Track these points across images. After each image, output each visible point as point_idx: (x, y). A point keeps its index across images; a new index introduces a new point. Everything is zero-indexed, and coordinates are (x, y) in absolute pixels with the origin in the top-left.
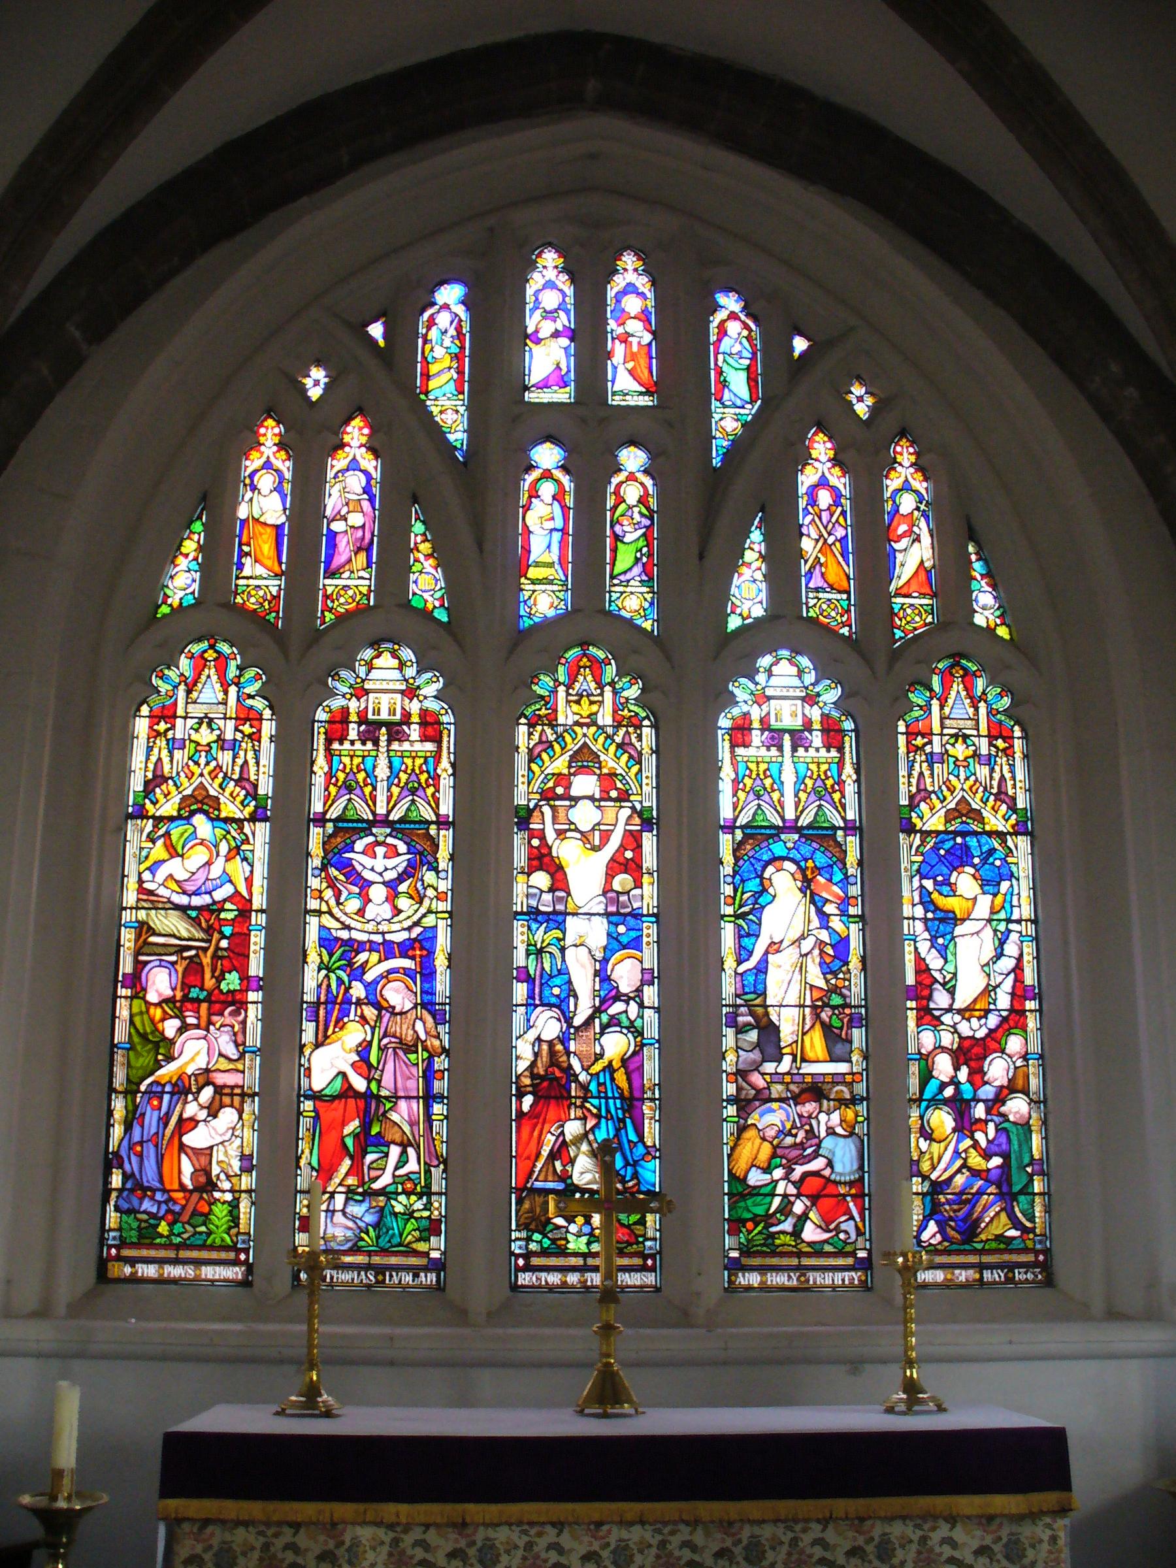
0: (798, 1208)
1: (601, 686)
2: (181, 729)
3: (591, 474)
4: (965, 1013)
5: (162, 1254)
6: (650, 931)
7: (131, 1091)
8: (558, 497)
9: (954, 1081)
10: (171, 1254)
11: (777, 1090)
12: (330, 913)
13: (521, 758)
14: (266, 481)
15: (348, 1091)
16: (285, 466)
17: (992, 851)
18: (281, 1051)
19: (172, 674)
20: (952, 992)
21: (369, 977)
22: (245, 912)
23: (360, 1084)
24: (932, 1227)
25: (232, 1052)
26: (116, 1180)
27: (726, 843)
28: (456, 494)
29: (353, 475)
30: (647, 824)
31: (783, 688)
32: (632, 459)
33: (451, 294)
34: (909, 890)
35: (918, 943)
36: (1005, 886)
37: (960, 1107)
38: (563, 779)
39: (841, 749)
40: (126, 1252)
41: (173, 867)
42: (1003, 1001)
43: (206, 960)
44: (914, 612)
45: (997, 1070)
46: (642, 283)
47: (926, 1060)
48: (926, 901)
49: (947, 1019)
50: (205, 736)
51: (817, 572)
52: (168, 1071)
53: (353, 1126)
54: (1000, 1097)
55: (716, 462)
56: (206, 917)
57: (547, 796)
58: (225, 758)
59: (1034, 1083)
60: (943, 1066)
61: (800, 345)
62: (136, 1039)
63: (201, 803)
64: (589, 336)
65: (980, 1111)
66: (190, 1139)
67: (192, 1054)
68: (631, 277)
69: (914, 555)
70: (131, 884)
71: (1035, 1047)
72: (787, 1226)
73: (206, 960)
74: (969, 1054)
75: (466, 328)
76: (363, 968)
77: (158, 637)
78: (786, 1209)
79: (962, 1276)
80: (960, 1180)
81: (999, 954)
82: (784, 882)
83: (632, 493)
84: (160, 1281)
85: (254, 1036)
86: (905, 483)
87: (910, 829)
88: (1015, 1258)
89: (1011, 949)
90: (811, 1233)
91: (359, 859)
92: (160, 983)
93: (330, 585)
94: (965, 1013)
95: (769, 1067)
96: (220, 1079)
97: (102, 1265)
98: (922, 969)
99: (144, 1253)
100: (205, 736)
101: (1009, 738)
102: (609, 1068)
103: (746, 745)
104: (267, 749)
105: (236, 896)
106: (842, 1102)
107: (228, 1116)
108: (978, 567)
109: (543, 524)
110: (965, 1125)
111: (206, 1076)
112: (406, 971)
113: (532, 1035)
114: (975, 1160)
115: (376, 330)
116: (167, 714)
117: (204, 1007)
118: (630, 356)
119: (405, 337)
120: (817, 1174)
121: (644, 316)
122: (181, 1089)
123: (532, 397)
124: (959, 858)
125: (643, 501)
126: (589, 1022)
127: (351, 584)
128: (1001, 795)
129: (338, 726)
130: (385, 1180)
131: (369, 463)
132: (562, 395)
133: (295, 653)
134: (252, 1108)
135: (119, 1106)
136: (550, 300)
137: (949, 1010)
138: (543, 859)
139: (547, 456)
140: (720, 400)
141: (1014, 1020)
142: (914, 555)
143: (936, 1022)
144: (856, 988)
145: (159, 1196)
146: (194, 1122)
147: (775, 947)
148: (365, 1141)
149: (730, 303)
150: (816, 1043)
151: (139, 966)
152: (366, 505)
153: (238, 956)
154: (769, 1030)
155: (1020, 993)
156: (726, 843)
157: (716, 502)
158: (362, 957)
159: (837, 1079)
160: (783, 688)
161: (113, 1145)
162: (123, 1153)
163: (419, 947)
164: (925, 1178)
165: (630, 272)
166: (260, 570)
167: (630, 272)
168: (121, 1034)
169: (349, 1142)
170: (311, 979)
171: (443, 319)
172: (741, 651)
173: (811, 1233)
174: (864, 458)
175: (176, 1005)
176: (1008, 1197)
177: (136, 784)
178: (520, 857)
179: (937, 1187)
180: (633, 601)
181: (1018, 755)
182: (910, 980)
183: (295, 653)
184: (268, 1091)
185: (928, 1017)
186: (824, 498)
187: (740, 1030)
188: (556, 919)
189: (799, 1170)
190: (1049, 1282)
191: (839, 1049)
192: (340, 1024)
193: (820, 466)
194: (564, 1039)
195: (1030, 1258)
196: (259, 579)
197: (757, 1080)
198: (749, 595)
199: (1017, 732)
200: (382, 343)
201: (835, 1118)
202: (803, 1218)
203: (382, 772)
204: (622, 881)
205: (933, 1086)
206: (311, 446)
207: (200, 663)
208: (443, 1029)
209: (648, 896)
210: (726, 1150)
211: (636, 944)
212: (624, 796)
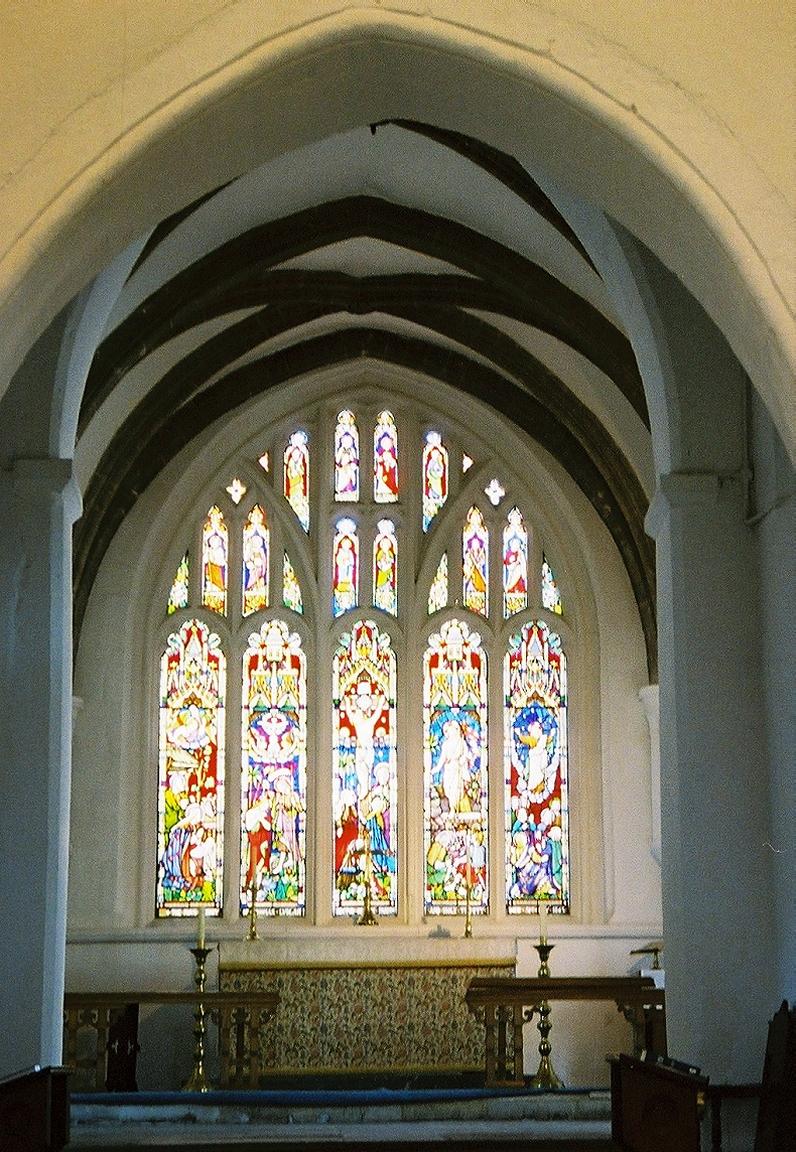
1: (371, 640)
2: (183, 665)
3: (367, 533)
5: (182, 905)
6: (393, 753)
7: (167, 833)
8: (352, 548)
10: (187, 905)
11: (449, 825)
12: (252, 749)
13: (336, 677)
14: (215, 542)
15: (262, 828)
16: (225, 535)
17: (548, 716)
18: (230, 812)
19: (177, 638)
22: (215, 748)
23: (267, 826)
25: (212, 814)
26: (162, 873)
27: (427, 714)
28: (301, 548)
29: (256, 535)
30: (392, 706)
31: (455, 638)
32: (386, 527)
33: (299, 440)
34: (508, 733)
35: (510, 756)
36: (553, 731)
37: (530, 833)
38: (355, 686)
39: (479, 668)
40: (166, 905)
41: (181, 730)
42: (551, 787)
43: (198, 773)
44: (515, 601)
45: (547, 816)
46: (392, 431)
47: (514, 813)
48: (516, 739)
49: (525, 794)
50: (194, 669)
51: (470, 584)
52: (183, 823)
53: (264, 845)
54: (548, 829)
55: (425, 529)
56: (198, 754)
57: (348, 693)
58: (203, 679)
59: (565, 823)
60: (522, 816)
61: (467, 463)
62: (169, 809)
63: (193, 701)
64: (365, 463)
65: (538, 835)
66: (193, 853)
68: (386, 429)
69: (517, 571)
70: (163, 739)
71: (565, 806)
73: (198, 773)
74: (535, 810)
75: (307, 461)
77: (170, 621)
79: (529, 910)
81: (550, 763)
82: (452, 729)
83: (385, 546)
84: (183, 917)
85: (221, 807)
86: (516, 534)
87: (509, 705)
88: (553, 903)
89: (555, 761)
91: (263, 723)
92: (179, 782)
93: (247, 594)
96: (206, 826)
97: (157, 911)
98: (514, 771)
99: (175, 905)
100: (194, 669)
101: (558, 660)
103: (437, 666)
104: (223, 675)
105: (211, 744)
106: (476, 831)
107: (210, 840)
108: (548, 577)
109: (345, 561)
110: (532, 841)
114: (537, 858)
115: (264, 462)
116: (175, 658)
117: (199, 794)
118: (385, 473)
119: (277, 463)
121: (392, 451)
122: (189, 831)
123: (339, 497)
124: (533, 718)
125: (391, 549)
127: (257, 595)
128: (553, 688)
129: (254, 664)
131: (265, 534)
132: (353, 496)
133: (233, 626)
134: (221, 837)
135: (162, 839)
136: (347, 442)
138: (345, 722)
139: (346, 527)
140: (427, 494)
141: (557, 793)
142: (517, 571)
144: (483, 776)
145: (181, 880)
146: (195, 845)
147: (448, 761)
148: (269, 851)
149: (434, 439)
151: (169, 777)
152: (263, 555)
153: (212, 772)
154: (442, 797)
155: (558, 782)
156: (427, 714)
157: (428, 547)
160: (455, 638)
161: (160, 859)
162: (165, 862)
163: (292, 765)
165: (386, 423)
166: (215, 588)
167: (386, 423)
168: (162, 808)
169: (263, 853)
170: (245, 781)
171: (296, 454)
172: (433, 621)
174: (495, 520)
176: (550, 873)
177: (163, 693)
178: (336, 722)
179: (518, 870)
180: (385, 598)
181: (562, 668)
182: (508, 775)
183: (233, 626)
184: (227, 831)
185: (515, 792)
186: (476, 544)
188: (352, 750)
190: (568, 912)
191: (476, 807)
193: (474, 526)
196: (214, 594)
198: (438, 595)
199: (562, 658)
200: (267, 469)
203: (274, 684)
204: (381, 731)
205: (517, 824)
206: (235, 521)
207: (189, 633)
208: (303, 801)
209: (391, 740)
210: (426, 853)
211: (387, 760)
212: (381, 693)
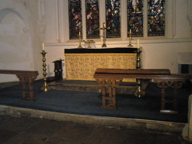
0: (136, 28)
4: (155, 5)
9: (154, 13)
20: (154, 2)
21: (92, 7)
23: (91, 18)
24: (151, 29)
49: (153, 5)
54: (159, 14)
66: (77, 25)
67: (76, 17)
72: (134, 30)
76: (92, 6)
78: (134, 28)
80: (154, 24)
90: (137, 31)
94: (155, 5)
95: (133, 13)
102: (116, 14)
111: (78, 19)
112: (95, 6)
113: (108, 12)
114: (156, 22)
120: (138, 24)
122: (76, 20)
126: (113, 9)
130: (95, 28)
137: (154, 4)
143: (152, 6)
146: (77, 24)
150: (138, 10)
158: (91, 5)
159: (140, 13)
164: (150, 24)
173: (137, 31)
175: (74, 12)
187: (129, 9)
189: (136, 24)
192: (90, 13)
194: (111, 12)
195: (162, 33)
197: (131, 14)
201: (140, 18)
202: (136, 29)
